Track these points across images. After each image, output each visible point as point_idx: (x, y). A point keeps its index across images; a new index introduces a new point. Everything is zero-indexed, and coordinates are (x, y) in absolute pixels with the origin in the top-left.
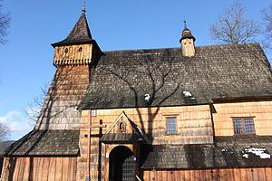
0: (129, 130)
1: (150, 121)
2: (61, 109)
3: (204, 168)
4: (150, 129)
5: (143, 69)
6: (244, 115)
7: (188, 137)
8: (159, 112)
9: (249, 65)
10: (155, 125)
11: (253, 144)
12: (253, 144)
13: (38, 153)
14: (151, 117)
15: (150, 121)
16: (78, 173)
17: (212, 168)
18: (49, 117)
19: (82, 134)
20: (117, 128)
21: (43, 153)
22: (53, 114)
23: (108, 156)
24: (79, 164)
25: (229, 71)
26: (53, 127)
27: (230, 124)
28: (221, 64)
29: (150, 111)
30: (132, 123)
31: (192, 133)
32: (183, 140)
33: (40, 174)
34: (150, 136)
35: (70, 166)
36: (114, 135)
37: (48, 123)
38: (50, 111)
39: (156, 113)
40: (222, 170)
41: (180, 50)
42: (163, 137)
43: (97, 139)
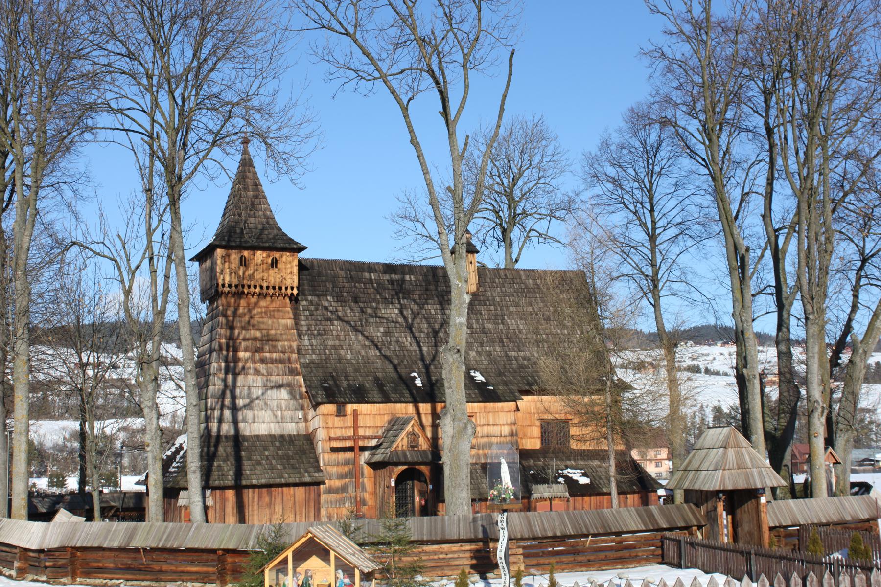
5: (392, 312)
7: (486, 452)
11: (568, 463)
12: (568, 463)
13: (254, 482)
16: (323, 512)
18: (234, 409)
20: (405, 441)
21: (263, 481)
22: (240, 402)
23: (393, 484)
24: (323, 497)
26: (247, 429)
27: (536, 431)
29: (434, 410)
31: (490, 445)
32: (478, 456)
33: (256, 517)
35: (307, 501)
36: (403, 451)
37: (235, 422)
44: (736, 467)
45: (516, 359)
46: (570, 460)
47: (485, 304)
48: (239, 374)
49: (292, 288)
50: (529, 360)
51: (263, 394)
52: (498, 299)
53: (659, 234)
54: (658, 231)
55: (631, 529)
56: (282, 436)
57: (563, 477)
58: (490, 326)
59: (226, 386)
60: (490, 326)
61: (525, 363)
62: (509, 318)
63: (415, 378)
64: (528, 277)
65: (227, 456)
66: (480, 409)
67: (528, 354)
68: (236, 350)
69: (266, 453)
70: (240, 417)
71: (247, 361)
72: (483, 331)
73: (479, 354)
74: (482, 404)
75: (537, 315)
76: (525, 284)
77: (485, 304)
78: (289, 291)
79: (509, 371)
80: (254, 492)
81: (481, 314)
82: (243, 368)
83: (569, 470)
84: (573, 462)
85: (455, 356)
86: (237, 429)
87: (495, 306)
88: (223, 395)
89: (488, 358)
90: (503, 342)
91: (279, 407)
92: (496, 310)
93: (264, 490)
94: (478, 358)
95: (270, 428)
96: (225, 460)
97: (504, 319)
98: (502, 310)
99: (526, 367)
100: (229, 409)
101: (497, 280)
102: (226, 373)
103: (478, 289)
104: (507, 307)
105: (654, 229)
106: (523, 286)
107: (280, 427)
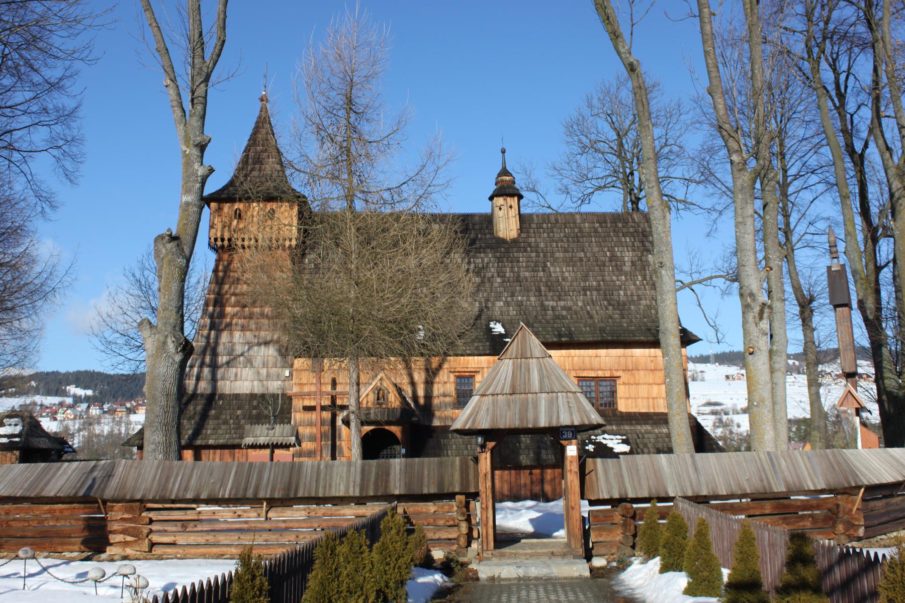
0: (393, 400)
1: (429, 383)
2: (239, 349)
3: (519, 467)
4: (429, 397)
6: (600, 374)
8: (446, 366)
9: (627, 267)
10: (437, 389)
13: (211, 442)
14: (431, 374)
15: (429, 383)
17: (531, 468)
18: (214, 366)
19: (297, 404)
20: (372, 398)
21: (221, 441)
22: (222, 359)
25: (585, 278)
26: (227, 387)
28: (570, 262)
30: (399, 390)
34: (427, 409)
37: (214, 380)
38: (215, 354)
39: (440, 366)
40: (549, 471)
41: (488, 220)
42: (449, 412)
43: (327, 415)
44: (507, 390)
45: (553, 308)
46: (611, 425)
47: (526, 251)
48: (223, 330)
49: (290, 240)
50: (569, 309)
51: (249, 350)
52: (542, 245)
53: (790, 183)
54: (789, 179)
55: (334, 493)
56: (263, 396)
57: (594, 443)
58: (527, 274)
59: (208, 342)
60: (527, 274)
61: (564, 313)
62: (552, 265)
63: (419, 329)
64: (584, 221)
65: (195, 414)
66: (489, 363)
67: (570, 303)
68: (223, 306)
69: (239, 412)
70: (219, 376)
71: (234, 316)
72: (518, 279)
73: (507, 304)
74: (491, 358)
75: (589, 260)
76: (580, 228)
77: (526, 251)
78: (287, 243)
79: (540, 322)
80: (215, 454)
81: (518, 261)
82: (229, 325)
83: (606, 436)
84: (614, 427)
85: (169, 246)
86: (214, 388)
87: (536, 252)
88: (204, 353)
89: (517, 308)
90: (540, 291)
91: (265, 365)
92: (538, 256)
93: (226, 451)
94: (505, 309)
95: (253, 386)
96: (190, 419)
97: (546, 266)
98: (545, 256)
99: (564, 318)
100: (209, 366)
101: (545, 226)
102: (211, 329)
103: (519, 235)
104: (553, 253)
105: (785, 176)
106: (576, 230)
107: (263, 386)
